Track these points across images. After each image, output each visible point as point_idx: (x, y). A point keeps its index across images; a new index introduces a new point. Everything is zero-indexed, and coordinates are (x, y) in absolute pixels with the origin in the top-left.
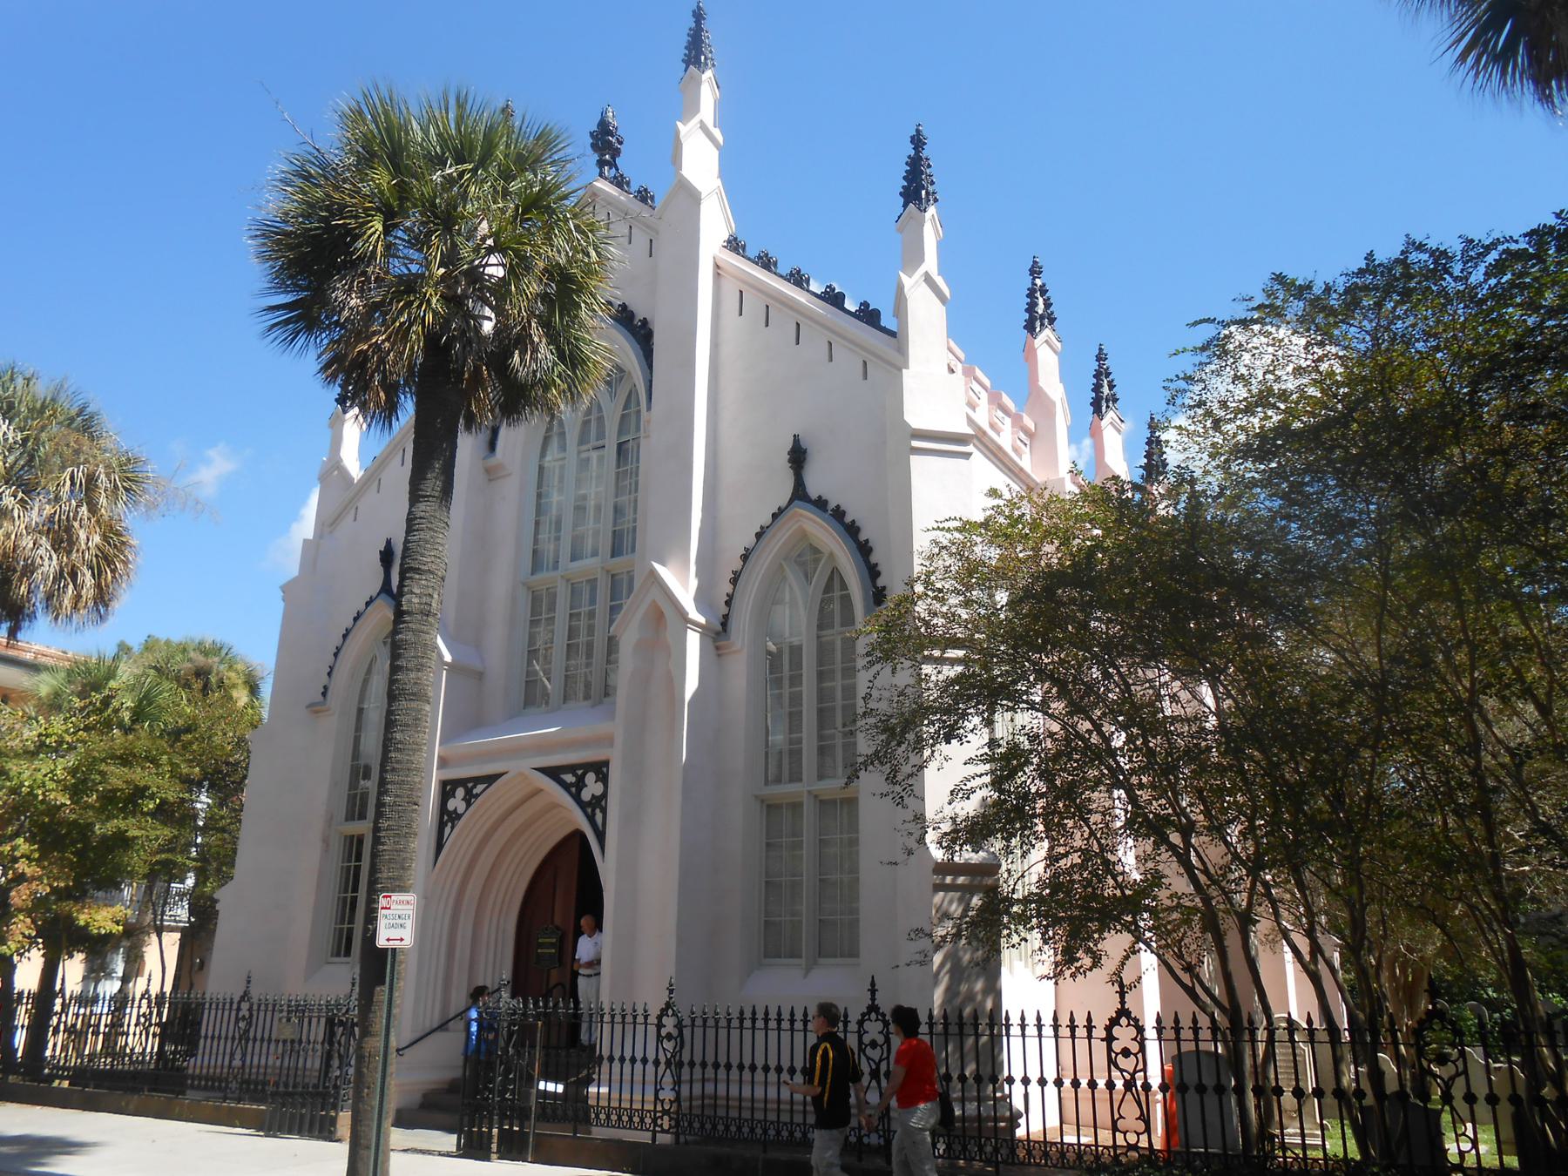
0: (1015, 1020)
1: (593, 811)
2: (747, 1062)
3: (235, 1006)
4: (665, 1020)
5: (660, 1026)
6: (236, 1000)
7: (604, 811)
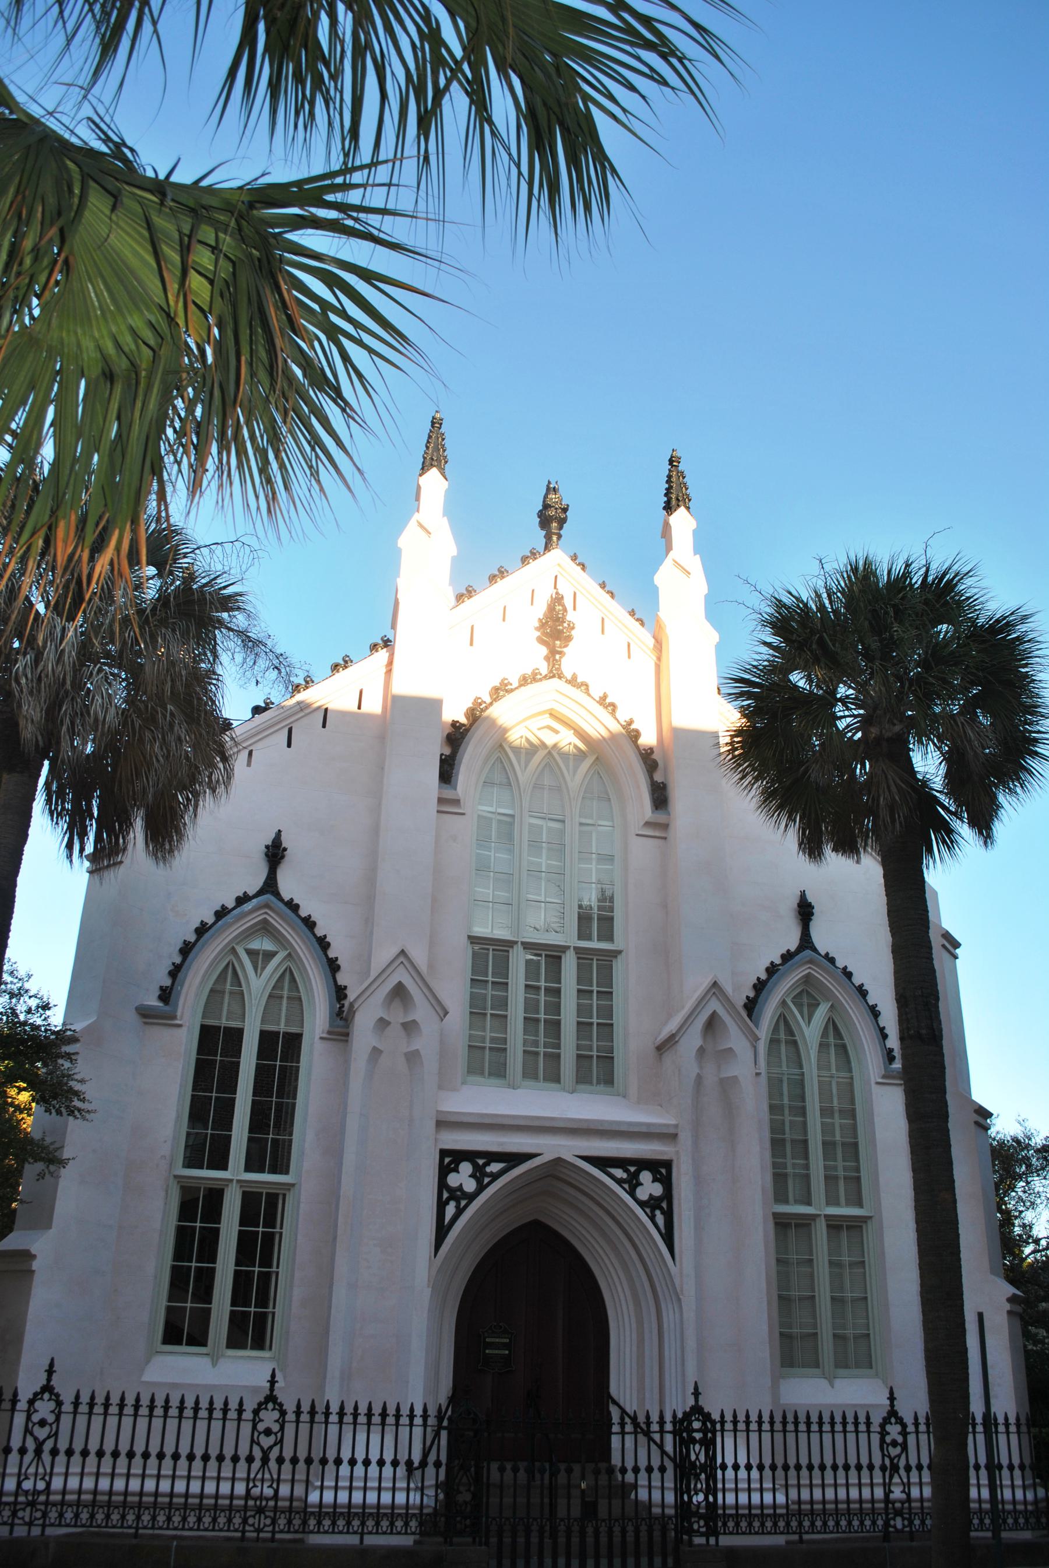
0: (1001, 1420)
1: (653, 1212)
3: (248, 1415)
4: (888, 1428)
5: (883, 1433)
6: (249, 1406)
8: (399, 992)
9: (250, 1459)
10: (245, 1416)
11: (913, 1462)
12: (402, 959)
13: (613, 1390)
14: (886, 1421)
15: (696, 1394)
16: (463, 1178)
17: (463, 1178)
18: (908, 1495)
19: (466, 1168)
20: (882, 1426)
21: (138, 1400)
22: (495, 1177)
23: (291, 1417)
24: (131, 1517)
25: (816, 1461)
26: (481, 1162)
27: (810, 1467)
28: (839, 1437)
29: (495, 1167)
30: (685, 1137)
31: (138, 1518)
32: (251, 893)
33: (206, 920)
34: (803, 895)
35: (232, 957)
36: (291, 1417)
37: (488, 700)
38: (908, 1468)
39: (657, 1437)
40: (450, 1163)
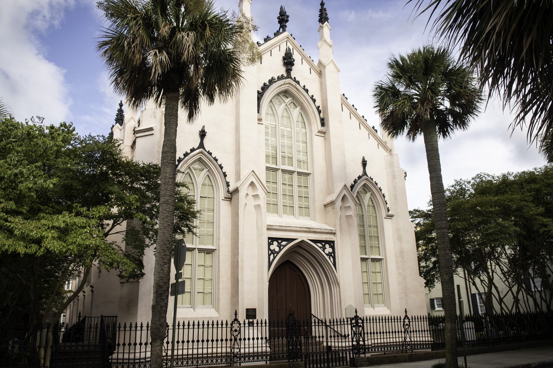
2: (375, 332)
3: (229, 326)
4: (405, 320)
5: (404, 322)
7: (334, 258)
8: (252, 184)
9: (231, 340)
10: (228, 326)
11: (412, 330)
12: (253, 173)
13: (313, 312)
14: (405, 318)
15: (356, 312)
16: (275, 246)
17: (275, 246)
18: (411, 339)
19: (275, 243)
20: (404, 320)
21: (194, 323)
22: (284, 246)
23: (242, 325)
24: (195, 362)
25: (415, 330)
26: (280, 241)
27: (386, 333)
28: (417, 323)
29: (284, 243)
30: (338, 233)
31: (197, 362)
32: (196, 148)
33: (181, 157)
34: (363, 158)
35: (188, 170)
36: (242, 325)
37: (268, 84)
38: (411, 332)
39: (332, 327)
40: (271, 242)
